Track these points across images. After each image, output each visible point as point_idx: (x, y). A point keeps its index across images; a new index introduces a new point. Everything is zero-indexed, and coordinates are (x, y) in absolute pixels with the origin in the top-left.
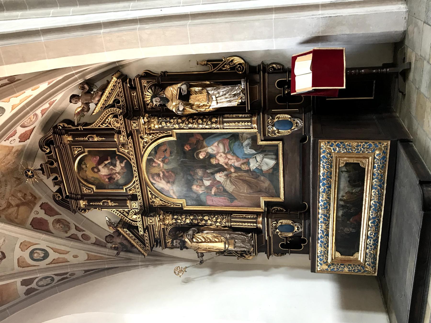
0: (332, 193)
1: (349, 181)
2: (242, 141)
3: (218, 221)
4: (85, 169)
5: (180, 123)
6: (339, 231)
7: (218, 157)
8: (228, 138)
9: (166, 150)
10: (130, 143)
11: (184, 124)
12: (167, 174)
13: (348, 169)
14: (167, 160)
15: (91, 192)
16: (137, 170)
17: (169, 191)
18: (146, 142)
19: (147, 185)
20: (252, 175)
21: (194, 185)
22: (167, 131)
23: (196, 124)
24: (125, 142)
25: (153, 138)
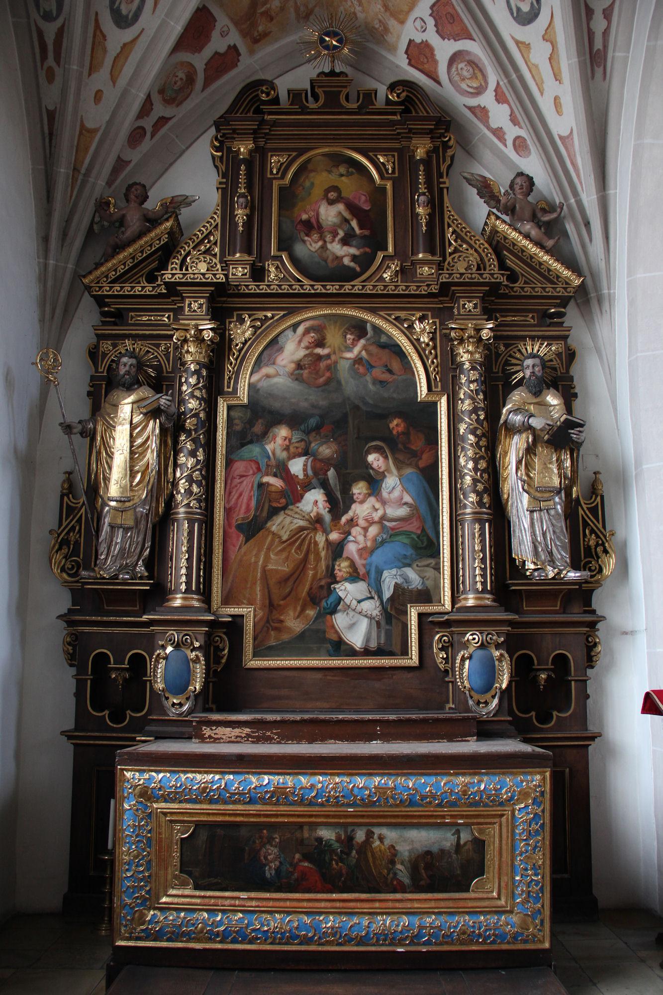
0: (390, 809)
1: (428, 853)
2: (417, 565)
4: (334, 170)
5: (478, 416)
6: (265, 831)
7: (372, 500)
8: (423, 530)
9: (390, 371)
10: (418, 287)
11: (476, 425)
12: (323, 365)
13: (466, 847)
14: (361, 370)
15: (271, 172)
16: (342, 291)
17: (274, 363)
18: (411, 327)
19: (291, 312)
20: (321, 587)
21: (290, 431)
23: (476, 454)
24: (418, 276)
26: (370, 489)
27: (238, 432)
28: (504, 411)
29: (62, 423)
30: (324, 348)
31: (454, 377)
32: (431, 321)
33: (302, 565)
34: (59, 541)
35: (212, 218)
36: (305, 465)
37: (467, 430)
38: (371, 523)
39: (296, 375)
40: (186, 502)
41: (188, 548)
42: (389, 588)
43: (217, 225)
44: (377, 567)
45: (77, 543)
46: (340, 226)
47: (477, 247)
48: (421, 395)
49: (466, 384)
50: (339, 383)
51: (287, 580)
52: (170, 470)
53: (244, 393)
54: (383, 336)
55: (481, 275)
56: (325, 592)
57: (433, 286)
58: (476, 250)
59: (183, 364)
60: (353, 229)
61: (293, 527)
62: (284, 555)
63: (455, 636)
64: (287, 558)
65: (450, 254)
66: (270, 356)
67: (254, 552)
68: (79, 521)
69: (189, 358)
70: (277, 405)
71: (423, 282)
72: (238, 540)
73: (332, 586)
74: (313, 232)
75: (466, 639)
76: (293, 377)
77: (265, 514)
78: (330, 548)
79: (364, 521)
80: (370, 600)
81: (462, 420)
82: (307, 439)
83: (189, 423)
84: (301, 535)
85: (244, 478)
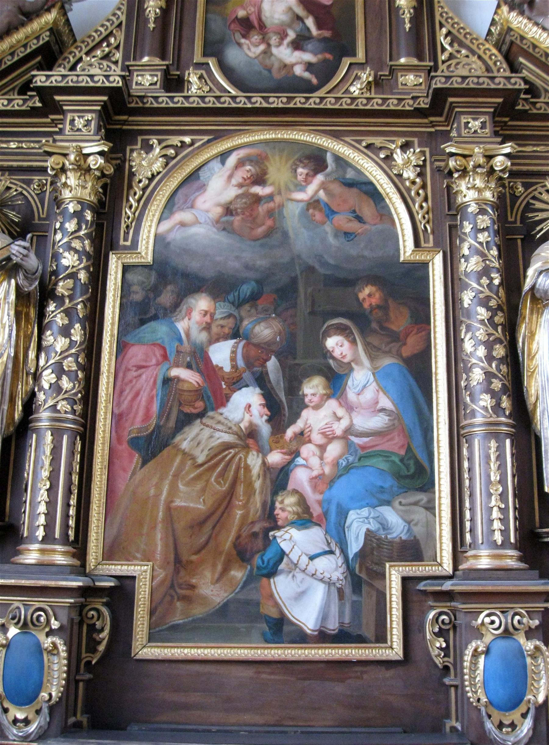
2: (400, 503)
3: (65, 378)
5: (491, 279)
7: (332, 404)
8: (409, 449)
9: (359, 219)
11: (487, 293)
12: (262, 209)
14: (318, 216)
16: (291, 105)
17: (192, 207)
18: (389, 158)
19: (218, 136)
20: (255, 535)
21: (213, 303)
22: (433, 232)
23: (489, 335)
24: (400, 86)
25: (408, 183)
26: (330, 388)
27: (137, 303)
28: (530, 272)
30: (264, 186)
31: (452, 228)
32: (418, 150)
33: (228, 498)
35: (114, 15)
36: (234, 352)
37: (475, 300)
38: (330, 438)
39: (223, 223)
41: (51, 472)
42: (357, 537)
43: (121, 24)
44: (339, 505)
46: (290, 26)
47: (481, 53)
48: (405, 252)
49: (472, 234)
50: (285, 234)
51: (201, 523)
52: (32, 355)
53: (147, 248)
54: (349, 170)
55: (492, 78)
56: (260, 543)
57: (422, 99)
58: (480, 57)
60: (308, 29)
61: (214, 443)
62: (199, 486)
63: (460, 615)
64: (203, 490)
65: (443, 62)
66: (187, 196)
67: (155, 480)
69: (66, 194)
70: (194, 265)
71: (409, 94)
72: (131, 461)
73: (271, 533)
74: (252, 33)
75: (479, 621)
76: (218, 225)
77: (172, 423)
78: (268, 476)
79: (320, 436)
80: (327, 556)
81: (466, 286)
82: (236, 314)
83: (62, 288)
84: (226, 456)
85: (143, 370)
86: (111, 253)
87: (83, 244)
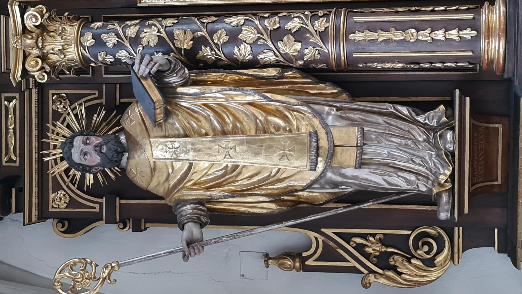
29: (184, 256)
34: (381, 271)
40: (317, 39)
45: (384, 241)
59: (85, 61)
68: (347, 238)
86: (139, 4)
87: (131, 25)
